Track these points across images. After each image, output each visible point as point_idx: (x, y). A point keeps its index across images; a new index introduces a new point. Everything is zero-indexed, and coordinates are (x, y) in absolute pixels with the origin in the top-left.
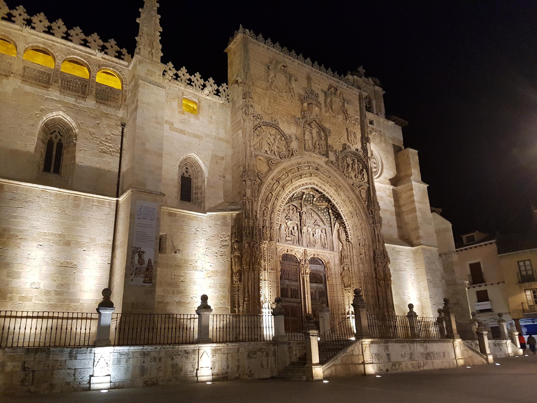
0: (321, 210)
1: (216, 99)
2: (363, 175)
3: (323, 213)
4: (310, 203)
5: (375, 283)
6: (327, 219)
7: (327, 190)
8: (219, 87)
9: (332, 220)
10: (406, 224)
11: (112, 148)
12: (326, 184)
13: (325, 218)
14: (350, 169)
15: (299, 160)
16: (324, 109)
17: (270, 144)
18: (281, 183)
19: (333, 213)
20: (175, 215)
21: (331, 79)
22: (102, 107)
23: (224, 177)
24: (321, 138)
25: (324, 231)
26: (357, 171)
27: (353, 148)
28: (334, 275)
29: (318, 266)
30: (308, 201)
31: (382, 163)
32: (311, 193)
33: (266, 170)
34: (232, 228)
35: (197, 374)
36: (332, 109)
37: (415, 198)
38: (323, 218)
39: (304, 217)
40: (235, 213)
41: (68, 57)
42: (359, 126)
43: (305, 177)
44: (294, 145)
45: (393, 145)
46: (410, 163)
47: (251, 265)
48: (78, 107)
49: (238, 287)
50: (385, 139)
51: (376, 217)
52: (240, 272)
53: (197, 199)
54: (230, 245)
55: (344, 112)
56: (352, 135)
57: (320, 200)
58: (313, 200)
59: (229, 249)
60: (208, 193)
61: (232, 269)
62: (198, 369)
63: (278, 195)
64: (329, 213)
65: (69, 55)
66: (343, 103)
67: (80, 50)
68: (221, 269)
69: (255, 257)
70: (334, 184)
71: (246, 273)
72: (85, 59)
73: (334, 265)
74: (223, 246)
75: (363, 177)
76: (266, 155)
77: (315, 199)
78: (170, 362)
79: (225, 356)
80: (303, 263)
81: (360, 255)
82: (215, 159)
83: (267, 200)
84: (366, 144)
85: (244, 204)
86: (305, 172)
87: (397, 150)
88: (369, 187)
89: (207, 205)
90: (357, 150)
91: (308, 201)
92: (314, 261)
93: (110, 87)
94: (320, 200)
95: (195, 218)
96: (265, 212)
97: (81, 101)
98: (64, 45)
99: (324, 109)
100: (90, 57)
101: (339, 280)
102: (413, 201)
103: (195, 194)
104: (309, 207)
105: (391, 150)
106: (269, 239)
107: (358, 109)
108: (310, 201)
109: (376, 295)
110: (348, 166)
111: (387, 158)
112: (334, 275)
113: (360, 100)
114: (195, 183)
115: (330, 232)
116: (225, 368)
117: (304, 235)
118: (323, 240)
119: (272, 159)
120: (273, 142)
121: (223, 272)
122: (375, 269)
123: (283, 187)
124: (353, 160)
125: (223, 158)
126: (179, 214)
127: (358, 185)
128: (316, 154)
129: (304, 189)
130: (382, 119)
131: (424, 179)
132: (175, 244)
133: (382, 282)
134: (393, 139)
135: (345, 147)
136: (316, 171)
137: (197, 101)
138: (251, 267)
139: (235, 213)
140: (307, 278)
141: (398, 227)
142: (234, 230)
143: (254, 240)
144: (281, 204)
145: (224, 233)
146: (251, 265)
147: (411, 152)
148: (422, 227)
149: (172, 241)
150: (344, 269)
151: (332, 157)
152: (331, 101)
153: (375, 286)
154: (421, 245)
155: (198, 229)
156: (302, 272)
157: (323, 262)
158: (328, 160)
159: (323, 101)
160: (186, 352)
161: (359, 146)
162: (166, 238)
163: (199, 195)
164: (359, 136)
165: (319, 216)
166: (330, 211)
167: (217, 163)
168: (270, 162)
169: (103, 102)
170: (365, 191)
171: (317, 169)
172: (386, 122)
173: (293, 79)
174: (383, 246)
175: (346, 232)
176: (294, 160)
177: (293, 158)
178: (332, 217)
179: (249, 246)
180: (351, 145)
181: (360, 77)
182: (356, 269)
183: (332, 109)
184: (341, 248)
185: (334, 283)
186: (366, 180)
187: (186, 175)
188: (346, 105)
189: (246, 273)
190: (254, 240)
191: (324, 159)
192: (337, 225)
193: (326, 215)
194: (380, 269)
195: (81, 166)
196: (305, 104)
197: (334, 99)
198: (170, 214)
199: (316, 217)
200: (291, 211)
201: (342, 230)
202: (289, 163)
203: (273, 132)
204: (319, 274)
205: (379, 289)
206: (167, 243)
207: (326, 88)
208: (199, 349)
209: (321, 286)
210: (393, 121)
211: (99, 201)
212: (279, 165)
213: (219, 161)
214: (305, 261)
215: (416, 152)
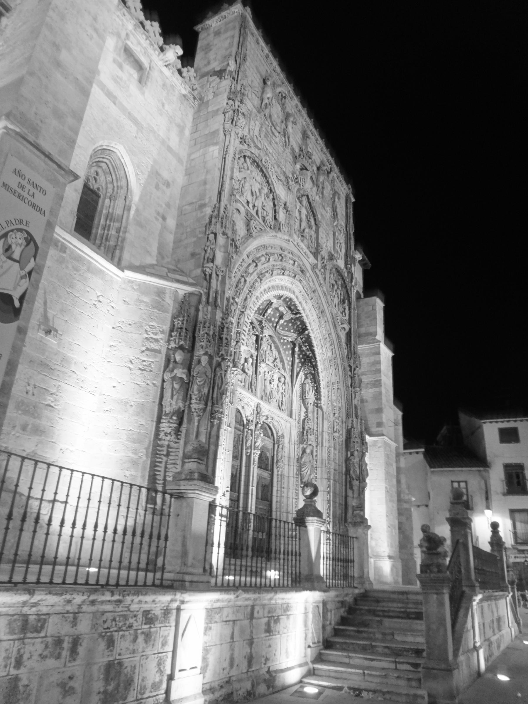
0: (283, 344)
1: (176, 79)
3: (285, 350)
5: (344, 484)
6: (289, 361)
7: (308, 312)
9: (296, 366)
12: (309, 301)
15: (284, 245)
17: (254, 194)
18: (260, 266)
19: (299, 355)
21: (324, 153)
23: (164, 218)
28: (287, 459)
30: (270, 321)
32: (282, 309)
34: (174, 317)
35: (168, 692)
39: (265, 346)
43: (289, 276)
47: (210, 404)
49: (168, 446)
52: (180, 416)
53: (107, 239)
58: (278, 323)
59: (161, 359)
60: (132, 234)
61: (161, 405)
62: (171, 678)
63: (253, 286)
64: (293, 352)
68: (137, 399)
73: (289, 443)
74: (147, 349)
75: (344, 311)
77: (281, 322)
78: (102, 658)
79: (228, 631)
80: (252, 427)
84: (351, 265)
85: (208, 278)
89: (126, 256)
94: (287, 326)
95: (99, 273)
101: (293, 470)
103: (104, 229)
108: (273, 322)
109: (343, 503)
114: (105, 205)
115: (290, 384)
116: (226, 664)
117: (260, 377)
120: (258, 194)
121: (141, 407)
122: (347, 460)
123: (261, 277)
126: (72, 252)
132: (51, 313)
133: (356, 483)
137: (146, 64)
138: (209, 408)
139: (183, 289)
140: (255, 456)
142: (178, 323)
143: (223, 352)
146: (210, 404)
149: (45, 303)
150: (304, 451)
153: (344, 487)
154: (383, 435)
155: (101, 299)
156: (249, 444)
157: (272, 434)
160: (149, 618)
163: (113, 232)
165: (279, 353)
166: (297, 349)
173: (291, 119)
175: (318, 391)
178: (297, 361)
179: (210, 363)
182: (325, 455)
183: (322, 193)
184: (303, 414)
186: (347, 317)
187: (93, 185)
189: (196, 419)
190: (223, 352)
193: (288, 356)
194: (356, 460)
196: (298, 166)
201: (309, 385)
203: (259, 177)
205: (350, 493)
208: (178, 610)
213: (161, 185)
214: (256, 426)
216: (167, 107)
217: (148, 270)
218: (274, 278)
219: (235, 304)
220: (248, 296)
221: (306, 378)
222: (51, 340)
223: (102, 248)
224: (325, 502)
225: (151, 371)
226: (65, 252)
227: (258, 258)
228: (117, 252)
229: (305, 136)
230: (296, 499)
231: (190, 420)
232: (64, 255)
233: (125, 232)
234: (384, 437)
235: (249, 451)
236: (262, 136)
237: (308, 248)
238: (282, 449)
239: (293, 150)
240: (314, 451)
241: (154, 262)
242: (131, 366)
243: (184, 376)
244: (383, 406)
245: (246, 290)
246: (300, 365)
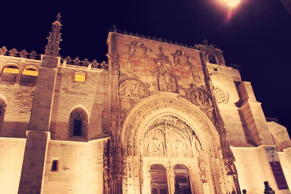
0: (181, 130)
2: (209, 102)
3: (183, 132)
4: (172, 126)
8: (100, 63)
9: (190, 136)
10: (250, 132)
11: (27, 109)
12: (179, 111)
13: (185, 135)
14: (197, 99)
15: (156, 98)
16: (173, 64)
20: (66, 145)
22: (23, 87)
24: (172, 82)
25: (185, 145)
26: (203, 100)
27: (199, 86)
29: (183, 170)
31: (228, 93)
32: (171, 119)
33: (129, 107)
36: (179, 63)
37: (253, 113)
38: (184, 135)
39: (167, 136)
40: (106, 139)
41: (7, 64)
42: (202, 72)
44: (152, 89)
45: (234, 81)
46: (246, 91)
47: (115, 175)
48: (9, 89)
50: (227, 78)
51: (221, 129)
52: (109, 181)
54: (103, 162)
55: (189, 65)
56: (197, 78)
57: (179, 123)
59: (102, 164)
61: (104, 179)
63: (140, 122)
65: (7, 63)
66: (188, 59)
67: (14, 60)
69: (117, 168)
70: (186, 110)
71: (112, 180)
72: (16, 63)
75: (209, 103)
76: (129, 98)
77: (174, 123)
80: (168, 169)
81: (212, 157)
82: (96, 106)
83: (131, 127)
84: (208, 81)
86: (161, 105)
87: (237, 84)
88: (214, 110)
89: (89, 136)
90: (202, 86)
91: (170, 125)
92: (178, 167)
93: (30, 76)
94: (179, 123)
96: (129, 136)
97: (11, 86)
98: (5, 58)
99: (173, 64)
100: (19, 62)
102: (252, 115)
104: (171, 129)
105: (233, 85)
106: (133, 155)
107: (200, 62)
110: (196, 97)
111: (231, 90)
112: (195, 175)
113: (200, 56)
117: (168, 149)
118: (184, 151)
119: (134, 100)
120: (134, 89)
124: (200, 93)
125: (102, 105)
126: (68, 145)
127: (205, 109)
128: (169, 92)
129: (164, 117)
130: (223, 67)
131: (258, 100)
134: (234, 78)
135: (192, 85)
136: (170, 103)
138: (115, 176)
139: (106, 139)
141: (245, 135)
143: (116, 156)
144: (142, 130)
145: (99, 154)
147: (246, 84)
148: (261, 132)
151: (182, 93)
152: (178, 59)
154: (261, 144)
156: (168, 176)
157: (186, 167)
158: (179, 95)
159: (173, 60)
161: (204, 84)
162: (59, 161)
163: (85, 130)
164: (202, 77)
167: (97, 108)
168: (132, 102)
169: (26, 84)
170: (211, 113)
171: (171, 102)
172: (226, 68)
174: (229, 149)
176: (152, 98)
177: (150, 97)
180: (196, 84)
181: (204, 45)
183: (179, 63)
185: (196, 181)
186: (211, 105)
187: (78, 119)
188: (190, 60)
190: (116, 156)
191: (176, 95)
192: (194, 138)
193: (186, 133)
195: (7, 122)
197: (180, 58)
198: (62, 145)
199: (177, 135)
200: (157, 133)
202: (148, 101)
203: (135, 82)
204: (183, 176)
206: (59, 165)
207: (174, 52)
209: (186, 184)
210: (232, 67)
211: (16, 142)
212: (139, 103)
215: (250, 83)
216: (96, 81)
217: (97, 137)
218: (152, 114)
219: (131, 133)
220: (138, 128)
221: (196, 139)
222: (67, 172)
223: (83, 137)
224: (213, 189)
225: (100, 169)
226: (66, 146)
227: (140, 112)
228: (86, 136)
229: (160, 49)
230: (203, 190)
231: (111, 182)
232: (66, 147)
233: (87, 129)
234: (262, 145)
235: (169, 178)
236: (133, 67)
237: (172, 92)
238: (191, 172)
239: (154, 59)
240: (206, 168)
241: (101, 132)
242: (95, 170)
243: (107, 168)
244: (258, 131)
245: (136, 126)
246: (193, 135)
